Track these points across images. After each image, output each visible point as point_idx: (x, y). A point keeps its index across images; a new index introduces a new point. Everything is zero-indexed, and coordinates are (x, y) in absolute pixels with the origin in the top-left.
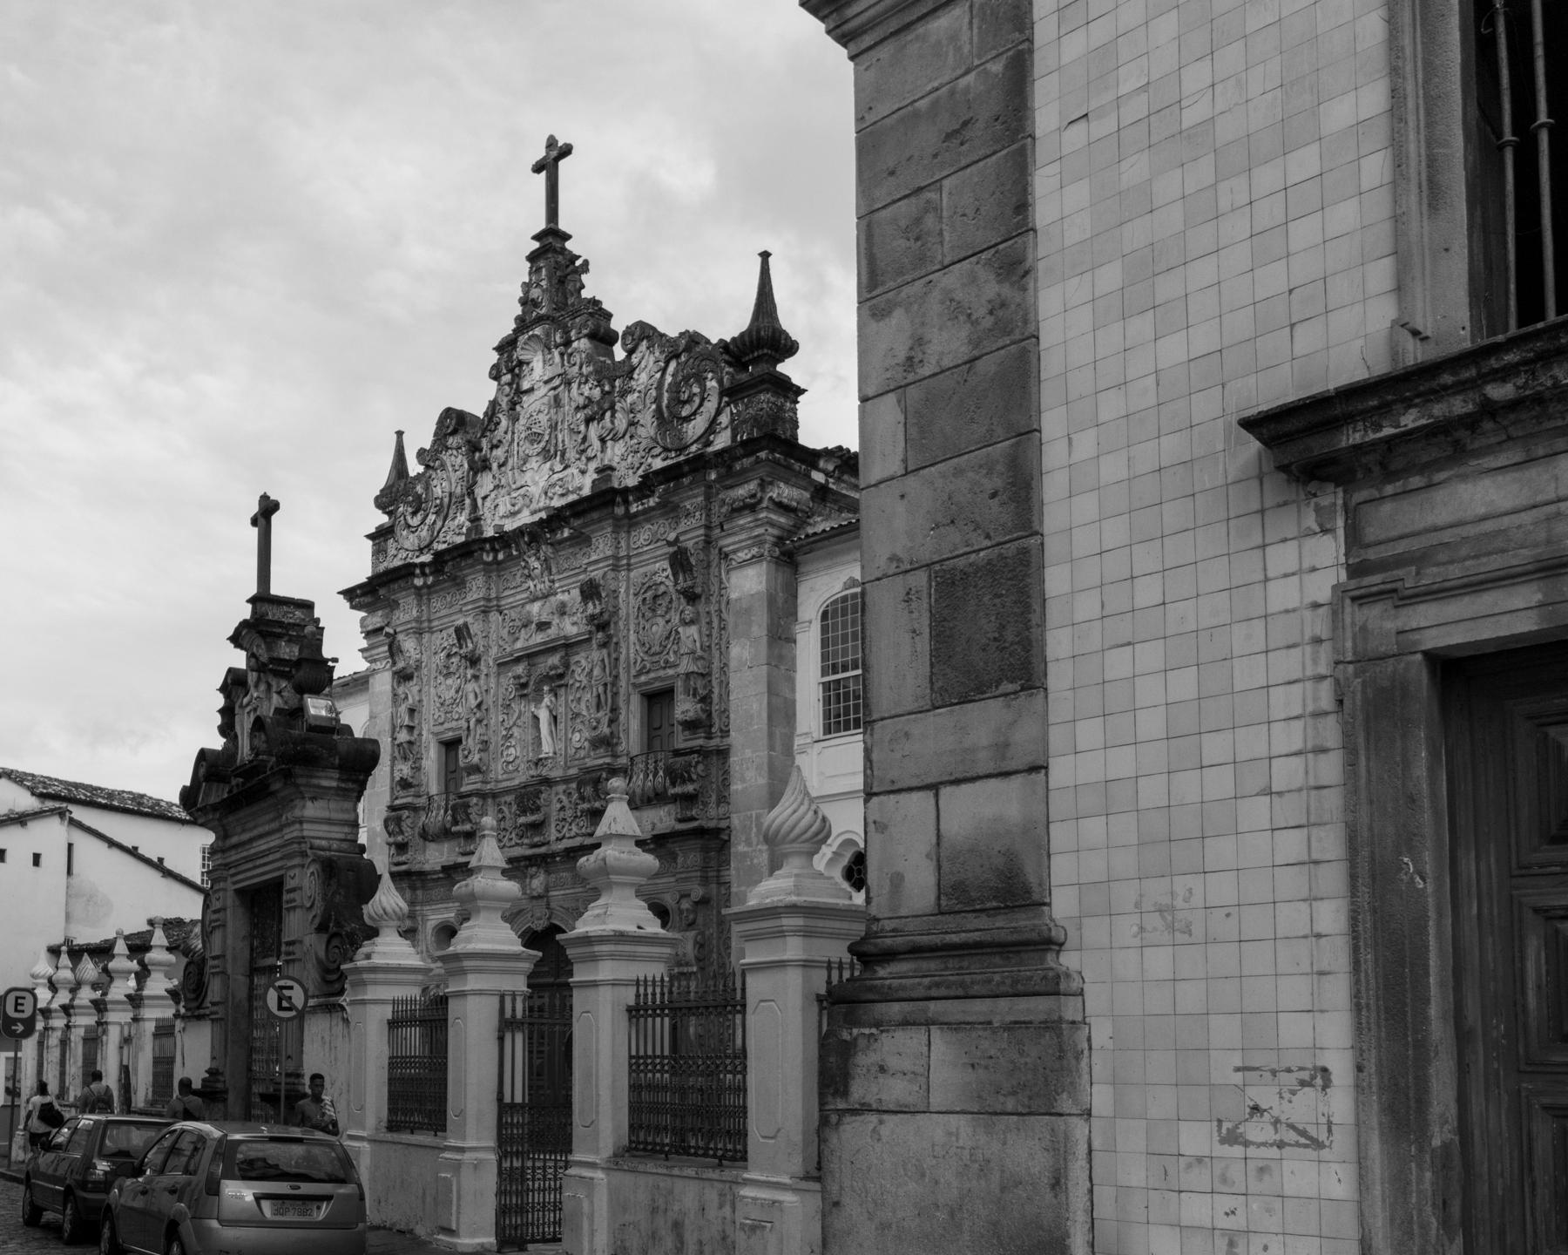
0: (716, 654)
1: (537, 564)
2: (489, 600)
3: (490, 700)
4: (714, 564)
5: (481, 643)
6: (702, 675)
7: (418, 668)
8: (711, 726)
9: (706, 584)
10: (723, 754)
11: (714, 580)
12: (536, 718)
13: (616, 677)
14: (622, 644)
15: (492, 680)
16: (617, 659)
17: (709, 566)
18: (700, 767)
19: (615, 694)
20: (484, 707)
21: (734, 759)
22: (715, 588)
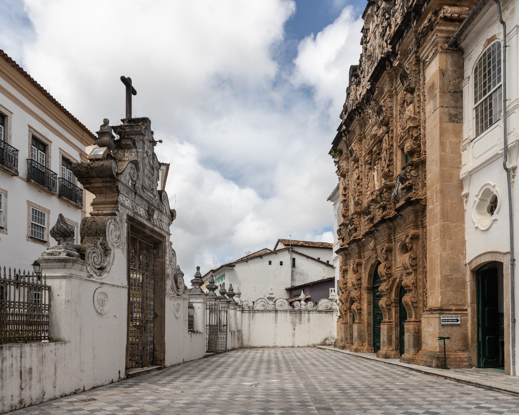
0: (422, 114)
1: (370, 111)
2: (361, 135)
3: (362, 176)
4: (421, 70)
5: (358, 153)
6: (416, 127)
7: (347, 172)
8: (420, 151)
9: (417, 82)
10: (423, 163)
11: (421, 78)
12: (374, 176)
13: (392, 145)
14: (395, 130)
15: (363, 166)
16: (392, 137)
17: (419, 72)
18: (413, 172)
19: (392, 153)
20: (360, 178)
21: (427, 163)
22: (421, 82)
